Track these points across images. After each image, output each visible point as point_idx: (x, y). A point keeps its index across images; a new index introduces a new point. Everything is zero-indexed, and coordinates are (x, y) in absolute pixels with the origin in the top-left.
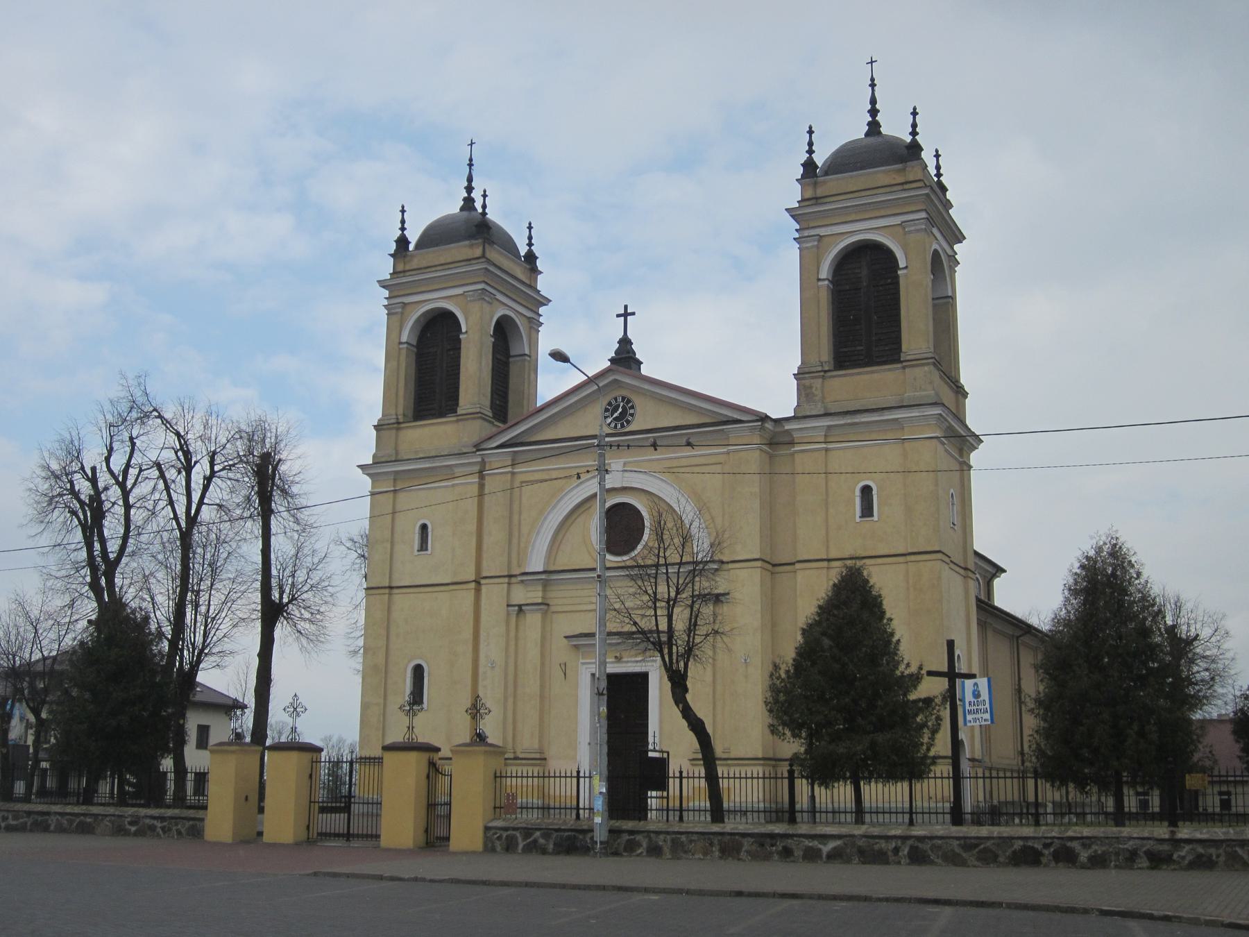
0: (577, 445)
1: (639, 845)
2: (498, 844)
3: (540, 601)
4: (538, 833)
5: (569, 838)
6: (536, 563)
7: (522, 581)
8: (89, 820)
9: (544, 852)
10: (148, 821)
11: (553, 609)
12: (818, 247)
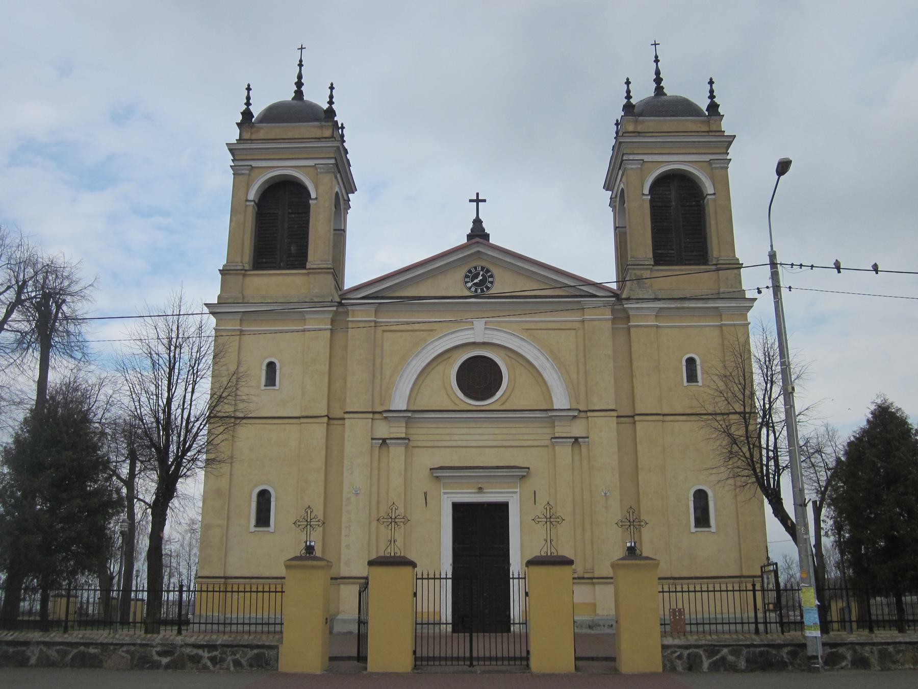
0: (443, 302)
1: (844, 658)
2: (678, 663)
3: (403, 436)
4: (725, 651)
5: (761, 653)
6: (399, 402)
7: (386, 418)
8: (92, 650)
9: (733, 669)
10: (188, 650)
11: (412, 444)
12: (641, 169)
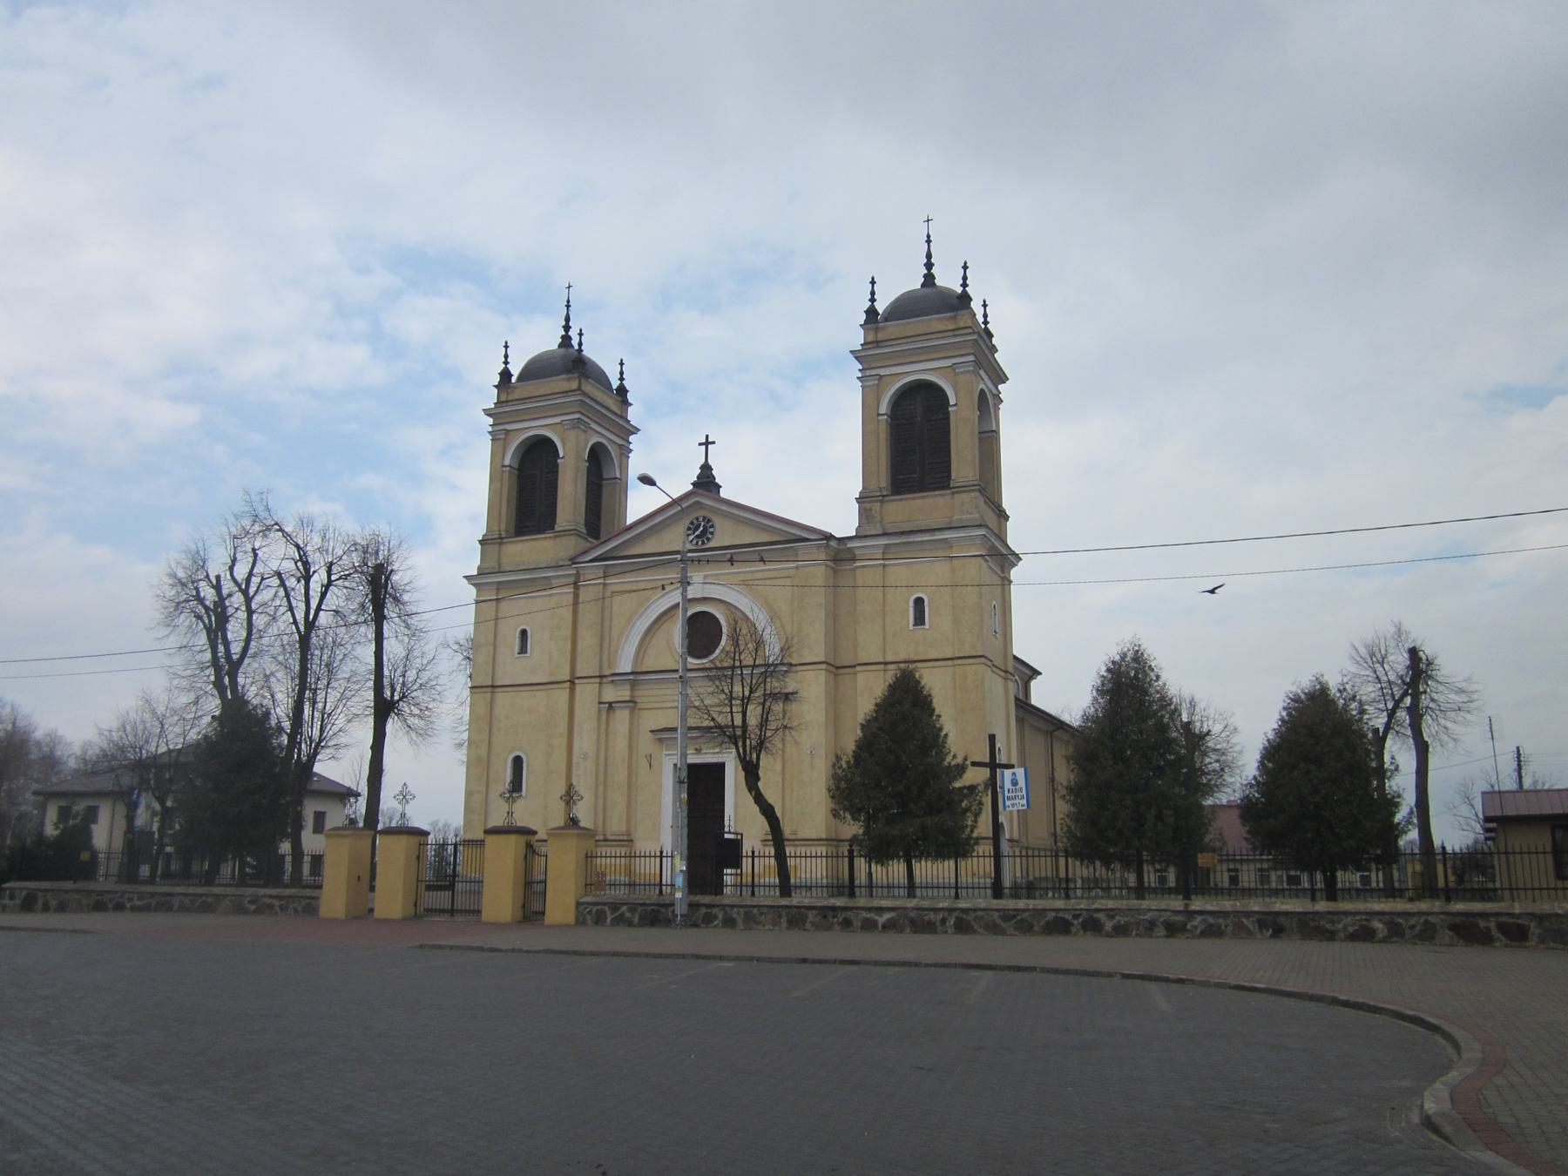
6: (625, 665)
9: (630, 924)
